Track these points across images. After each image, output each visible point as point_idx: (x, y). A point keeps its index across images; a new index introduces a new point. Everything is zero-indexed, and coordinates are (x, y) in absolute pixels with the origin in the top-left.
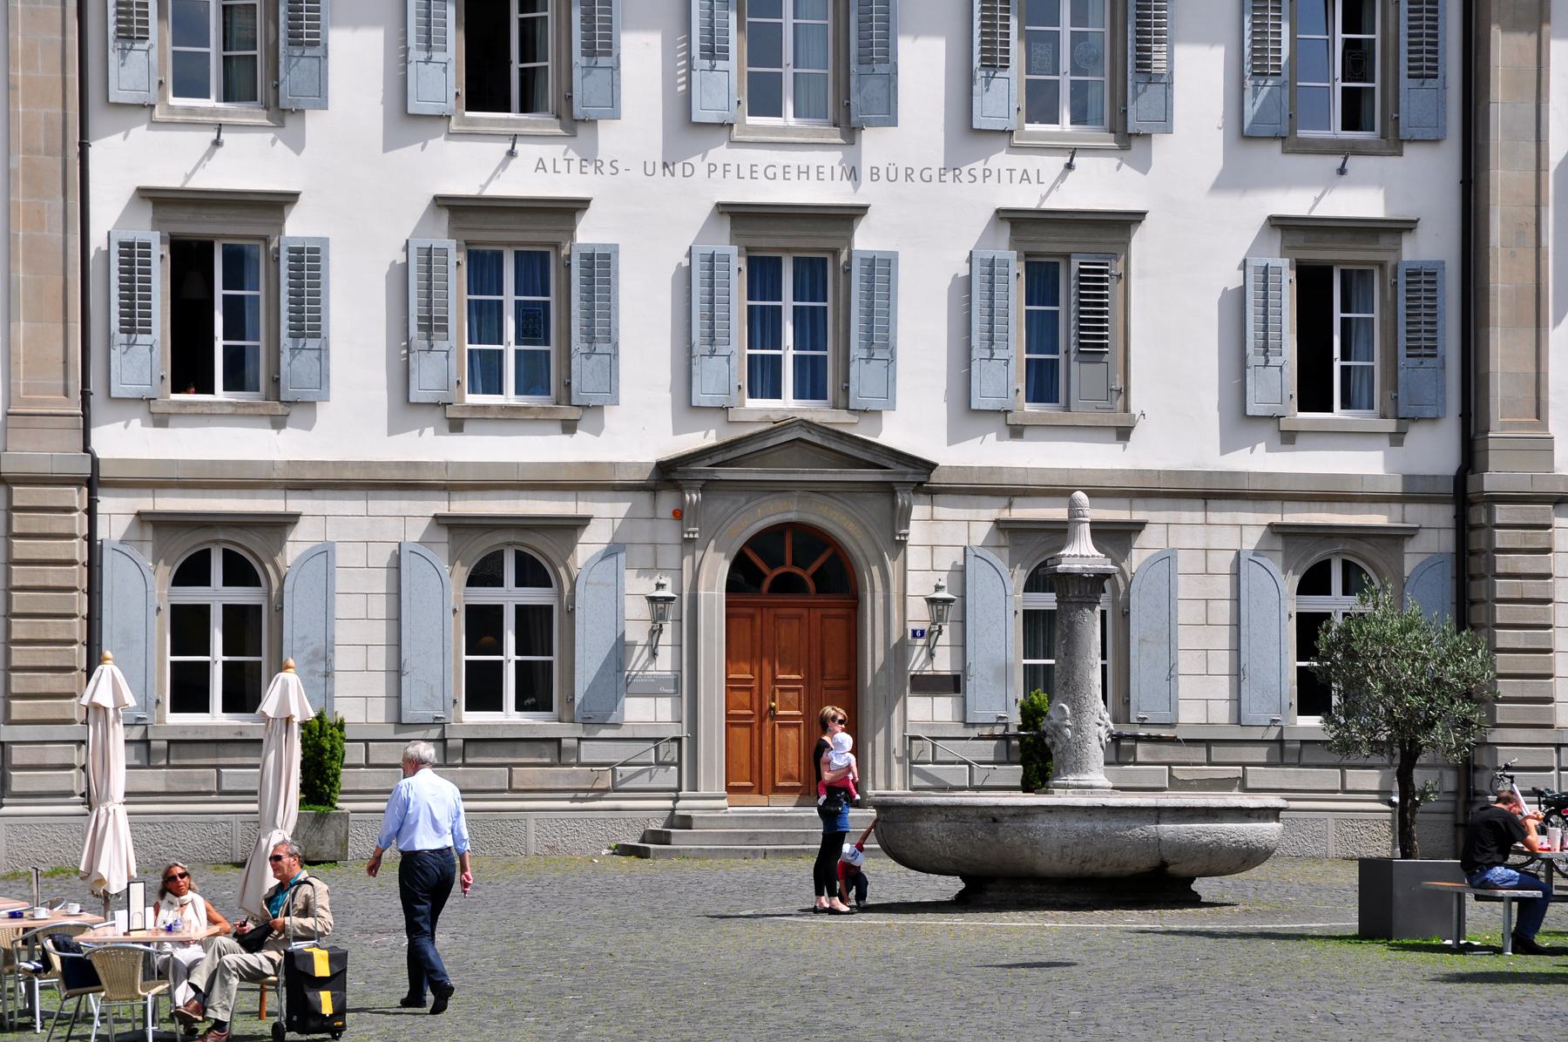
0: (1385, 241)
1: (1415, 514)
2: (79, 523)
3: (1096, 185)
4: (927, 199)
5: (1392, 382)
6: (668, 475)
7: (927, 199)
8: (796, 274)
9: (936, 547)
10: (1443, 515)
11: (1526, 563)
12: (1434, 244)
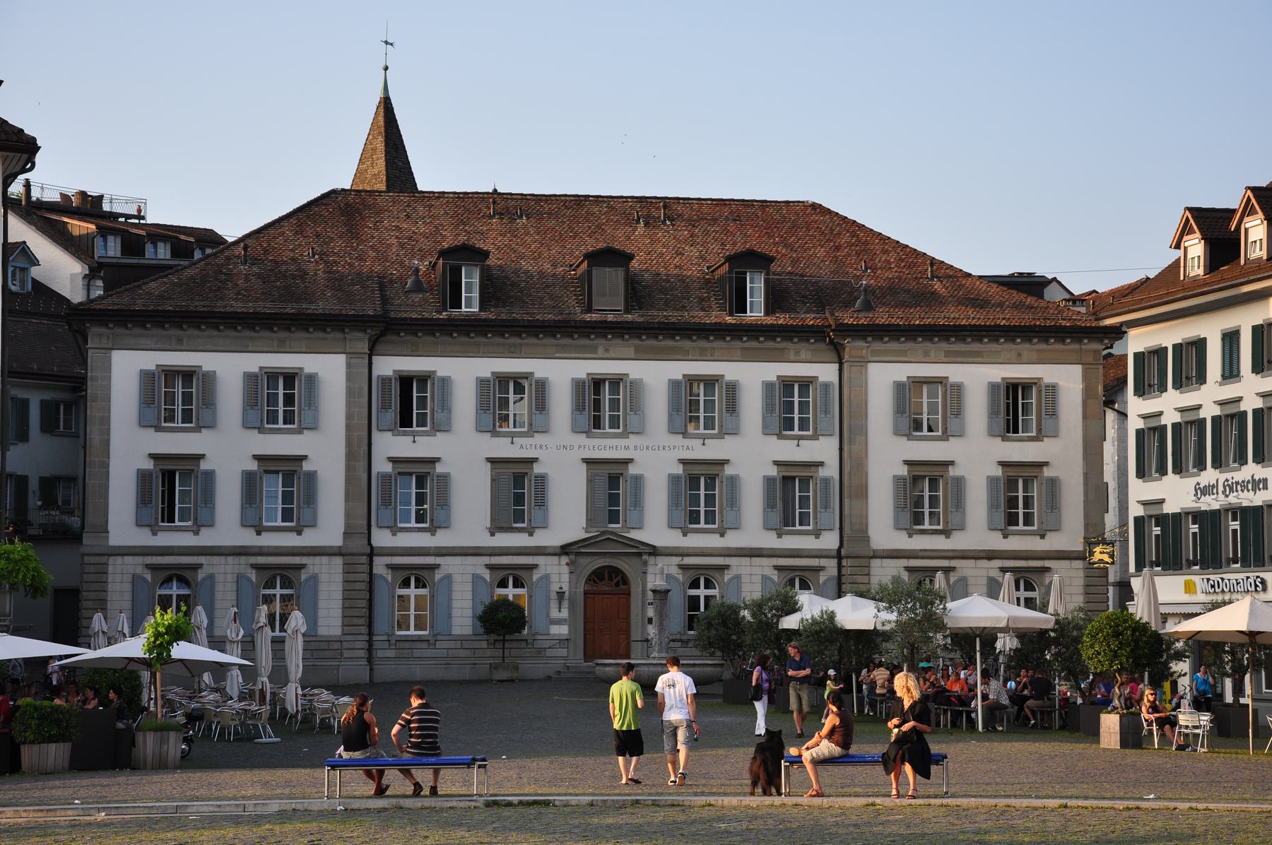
0: (813, 469)
1: (823, 562)
2: (366, 568)
4: (656, 455)
5: (815, 518)
6: (565, 550)
7: (656, 455)
8: (611, 485)
9: (657, 575)
10: (836, 561)
11: (859, 579)
12: (831, 471)
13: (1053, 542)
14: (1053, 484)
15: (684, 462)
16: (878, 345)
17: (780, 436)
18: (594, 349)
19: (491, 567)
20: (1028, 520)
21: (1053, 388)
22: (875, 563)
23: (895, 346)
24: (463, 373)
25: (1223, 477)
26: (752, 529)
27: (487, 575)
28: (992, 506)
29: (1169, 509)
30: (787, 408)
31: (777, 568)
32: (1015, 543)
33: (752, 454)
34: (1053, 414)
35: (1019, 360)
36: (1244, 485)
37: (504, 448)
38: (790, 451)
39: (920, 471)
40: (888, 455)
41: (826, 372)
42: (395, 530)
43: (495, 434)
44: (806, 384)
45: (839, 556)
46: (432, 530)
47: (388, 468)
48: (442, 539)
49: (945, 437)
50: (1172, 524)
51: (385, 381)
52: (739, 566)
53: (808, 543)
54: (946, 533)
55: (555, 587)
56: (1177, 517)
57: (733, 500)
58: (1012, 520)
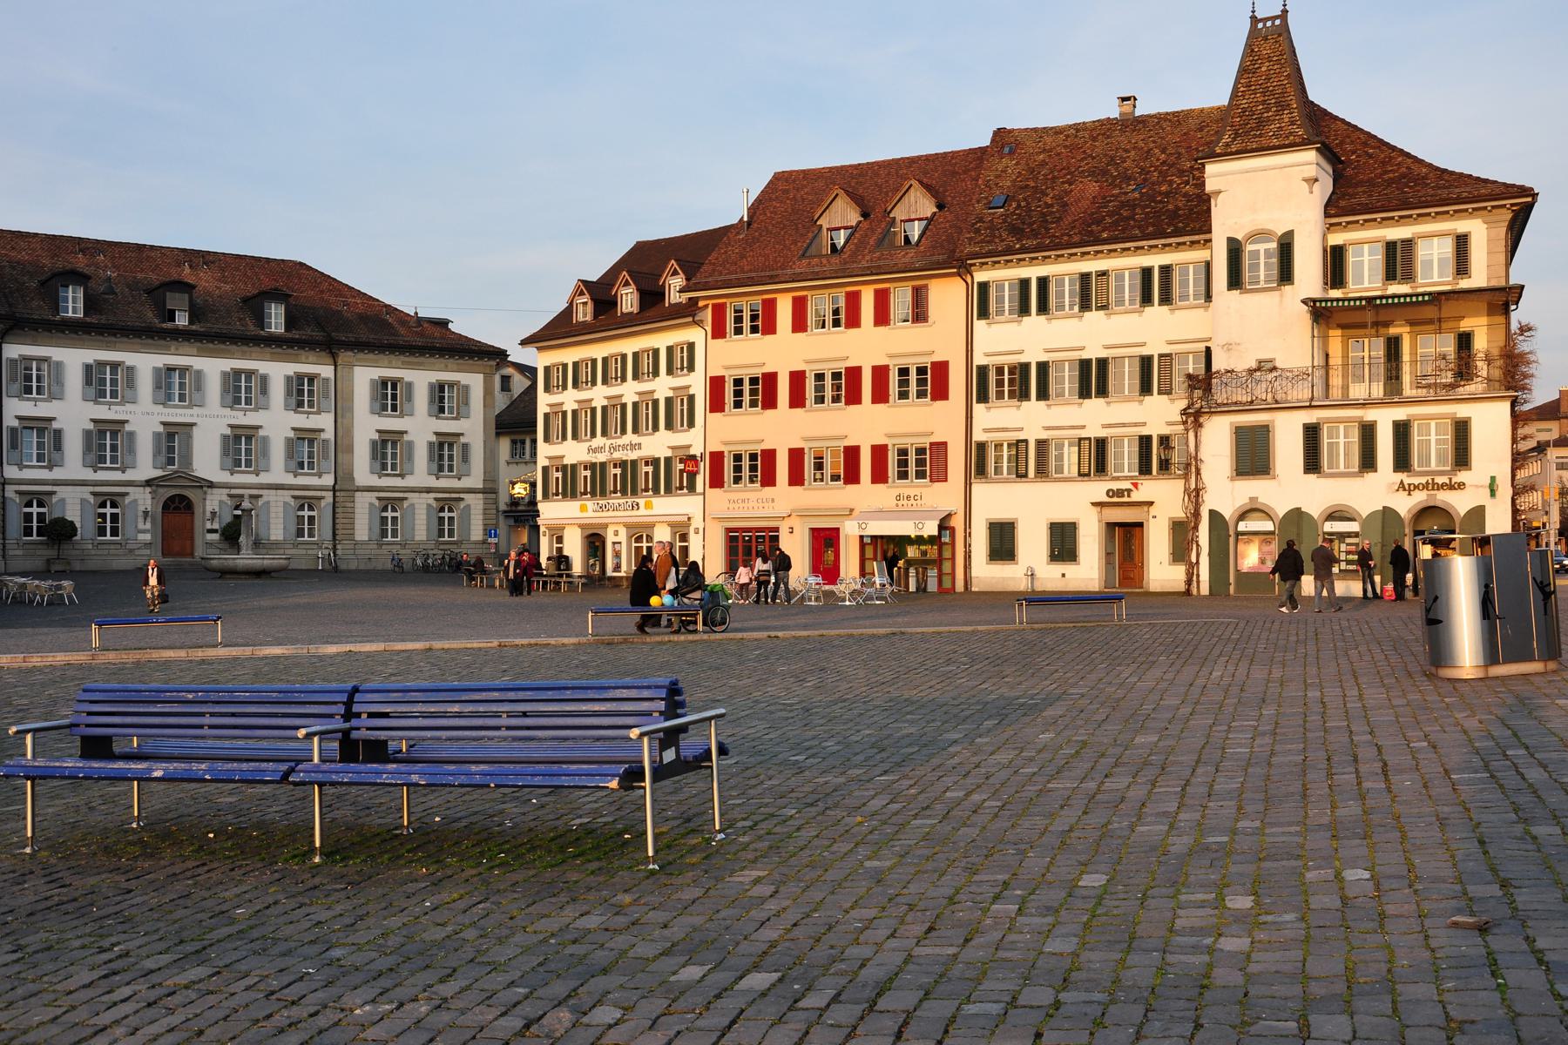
1: (323, 494)
3: (250, 419)
4: (210, 424)
6: (148, 483)
7: (210, 424)
9: (214, 501)
12: (329, 435)
13: (466, 483)
14: (465, 447)
15: (231, 426)
16: (361, 355)
17: (296, 411)
18: (168, 348)
19: (94, 494)
20: (451, 469)
21: (467, 387)
22: (358, 494)
23: (371, 356)
24: (73, 359)
25: (609, 442)
26: (277, 472)
27: (91, 499)
28: (431, 459)
29: (567, 461)
30: (300, 392)
31: (295, 497)
32: (443, 483)
33: (277, 422)
34: (467, 404)
35: (446, 369)
36: (624, 447)
37: (103, 412)
38: (302, 421)
39: (386, 437)
40: (366, 425)
41: (326, 371)
42: (21, 467)
43: (96, 402)
44: (312, 379)
45: (334, 490)
46: (50, 467)
47: (16, 423)
48: (57, 474)
49: (402, 416)
50: (569, 472)
51: (13, 361)
52: (268, 495)
53: (314, 481)
54: (402, 476)
55: (142, 508)
56: (574, 467)
57: (265, 453)
58: (441, 468)
